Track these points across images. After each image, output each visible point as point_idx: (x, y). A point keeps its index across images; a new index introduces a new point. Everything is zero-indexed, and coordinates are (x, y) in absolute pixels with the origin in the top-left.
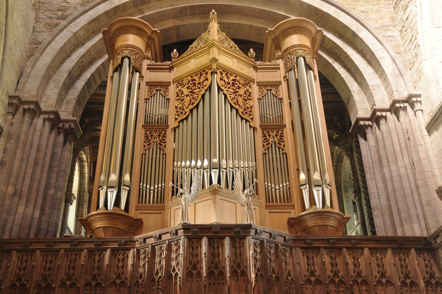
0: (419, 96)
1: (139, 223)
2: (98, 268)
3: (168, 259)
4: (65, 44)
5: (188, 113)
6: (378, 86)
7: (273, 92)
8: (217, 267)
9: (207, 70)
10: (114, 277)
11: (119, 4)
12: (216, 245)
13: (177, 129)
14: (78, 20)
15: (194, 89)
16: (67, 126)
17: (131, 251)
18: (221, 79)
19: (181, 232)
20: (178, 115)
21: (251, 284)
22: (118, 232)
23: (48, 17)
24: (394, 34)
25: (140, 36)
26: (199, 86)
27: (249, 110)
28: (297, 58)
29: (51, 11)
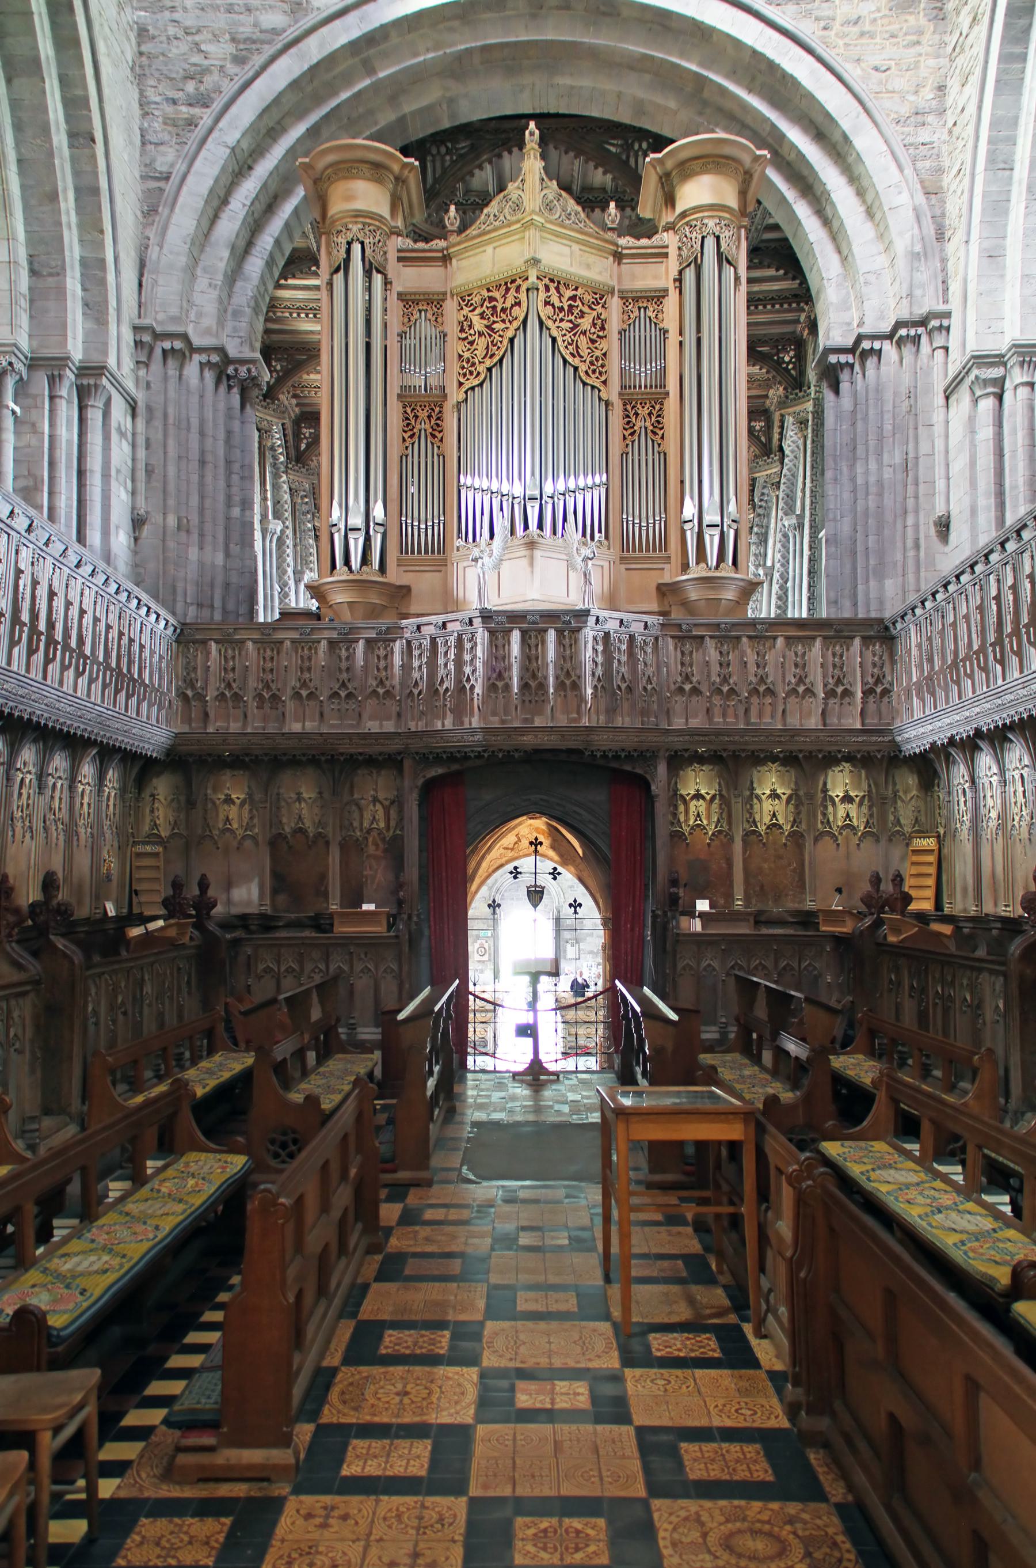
0: (948, 315)
1: (404, 591)
2: (348, 669)
3: (459, 662)
4: (217, 181)
5: (482, 376)
6: (878, 274)
7: (650, 313)
8: (534, 676)
9: (519, 281)
10: (374, 683)
11: (320, 57)
12: (533, 642)
13: (463, 405)
14: (234, 110)
15: (494, 322)
16: (243, 371)
17: (398, 643)
18: (547, 303)
19: (477, 622)
20: (465, 375)
21: (586, 703)
22: (374, 612)
23: (167, 99)
24: (935, 138)
25: (379, 181)
26: (504, 316)
27: (598, 365)
28: (703, 238)
29: (171, 79)
